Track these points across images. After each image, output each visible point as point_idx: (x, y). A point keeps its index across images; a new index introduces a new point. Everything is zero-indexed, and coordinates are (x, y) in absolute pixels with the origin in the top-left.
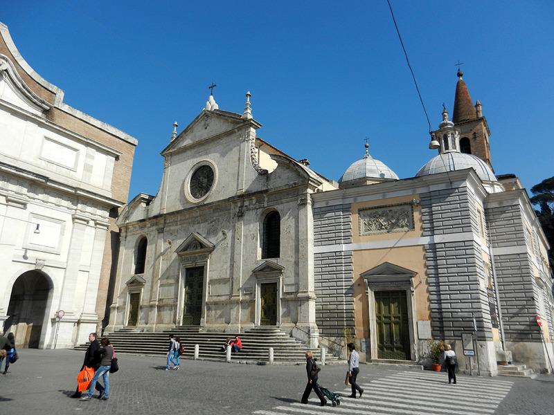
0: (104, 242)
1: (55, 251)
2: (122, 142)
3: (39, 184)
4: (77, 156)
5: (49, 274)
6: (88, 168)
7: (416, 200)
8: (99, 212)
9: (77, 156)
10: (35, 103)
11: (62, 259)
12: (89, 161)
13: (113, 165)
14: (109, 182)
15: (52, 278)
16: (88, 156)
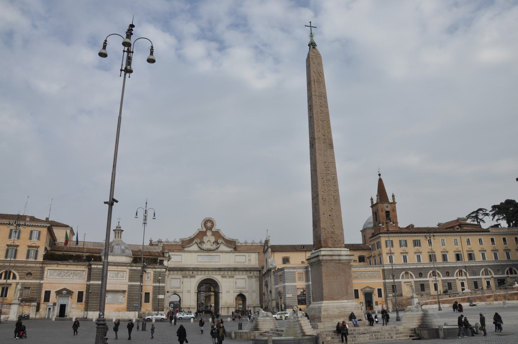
0: (259, 282)
1: (227, 293)
2: (259, 247)
3: (235, 270)
4: (246, 257)
5: (244, 294)
6: (250, 260)
7: (282, 274)
8: (255, 273)
9: (246, 257)
10: (231, 247)
11: (247, 289)
12: (249, 258)
13: (258, 256)
14: (257, 262)
15: (245, 295)
16: (249, 256)
